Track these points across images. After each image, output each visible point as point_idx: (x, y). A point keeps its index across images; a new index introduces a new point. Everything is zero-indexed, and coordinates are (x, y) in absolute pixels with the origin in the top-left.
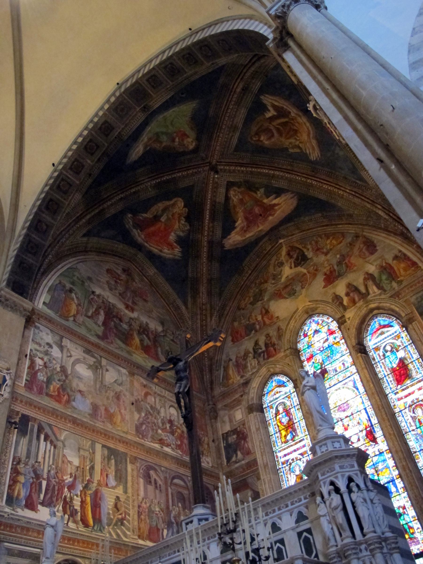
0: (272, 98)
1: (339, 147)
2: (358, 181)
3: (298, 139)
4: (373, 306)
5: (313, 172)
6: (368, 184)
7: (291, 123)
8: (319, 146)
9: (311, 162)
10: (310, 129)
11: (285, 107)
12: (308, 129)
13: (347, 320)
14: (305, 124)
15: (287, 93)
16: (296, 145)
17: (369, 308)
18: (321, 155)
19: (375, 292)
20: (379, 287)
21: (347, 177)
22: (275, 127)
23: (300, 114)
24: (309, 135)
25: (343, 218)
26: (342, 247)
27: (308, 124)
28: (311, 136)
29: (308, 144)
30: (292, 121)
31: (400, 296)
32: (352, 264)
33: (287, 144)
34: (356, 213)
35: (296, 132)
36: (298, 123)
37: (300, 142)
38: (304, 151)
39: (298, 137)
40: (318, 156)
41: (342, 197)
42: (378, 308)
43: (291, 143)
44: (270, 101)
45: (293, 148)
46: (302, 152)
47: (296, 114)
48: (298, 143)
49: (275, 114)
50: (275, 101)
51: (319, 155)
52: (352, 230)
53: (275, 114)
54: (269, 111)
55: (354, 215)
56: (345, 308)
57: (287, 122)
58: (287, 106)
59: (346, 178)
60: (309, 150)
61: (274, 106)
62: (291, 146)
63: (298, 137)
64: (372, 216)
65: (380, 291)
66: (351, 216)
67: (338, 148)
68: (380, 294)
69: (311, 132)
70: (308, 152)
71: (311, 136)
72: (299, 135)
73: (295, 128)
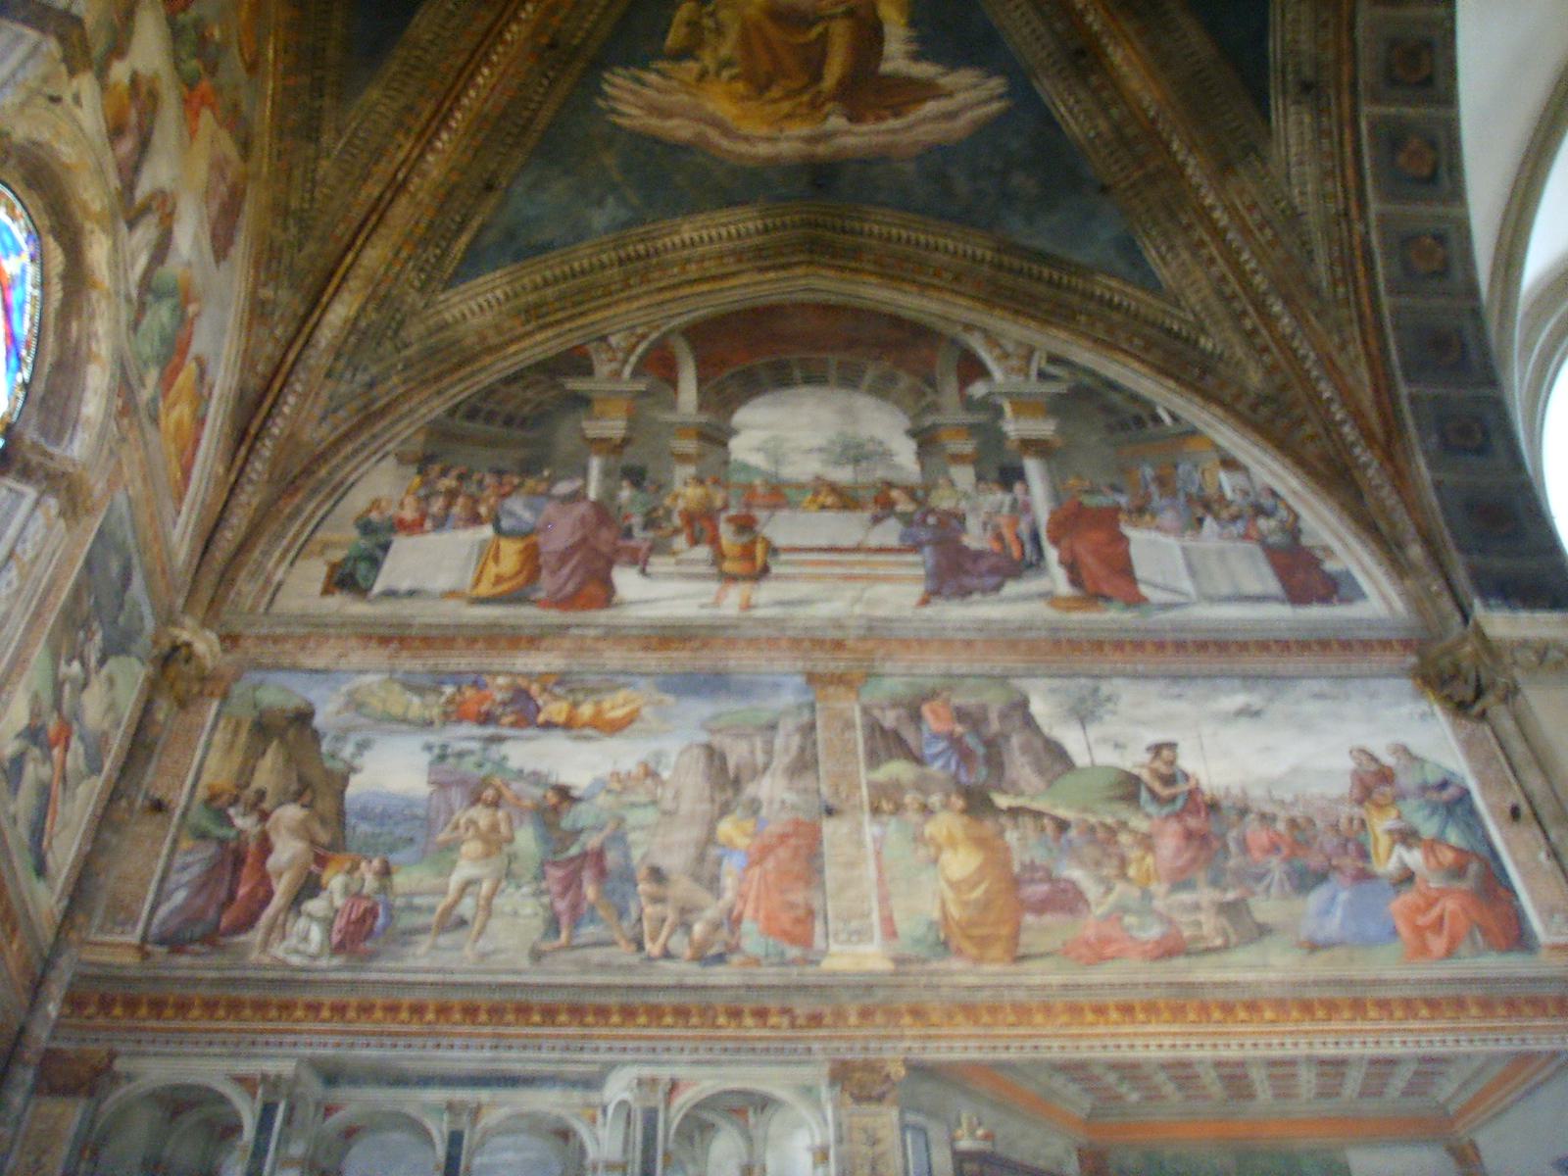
0: (970, 115)
1: (627, 225)
2: (465, 239)
3: (725, 74)
4: (98, 252)
5: (552, 46)
6: (448, 285)
7: (800, 91)
8: (657, 140)
9: (599, 65)
10: (742, 148)
11: (893, 123)
12: (747, 139)
13: (75, 83)
14: (769, 139)
15: (962, 185)
16: (700, 43)
17: (88, 226)
18: (619, 128)
19: (132, 266)
20: (146, 284)
21: (493, 200)
22: (822, 18)
23: (822, 150)
24: (716, 123)
25: (305, 80)
26: (233, 65)
27: (763, 150)
28: (713, 135)
29: (685, 98)
30: (806, 98)
31: (126, 421)
32: (197, 114)
33: (724, 15)
34: (325, 164)
35: (759, 86)
36: (789, 116)
37: (703, 75)
38: (661, 65)
39: (733, 78)
40: (621, 114)
41: (399, 124)
42: (75, 278)
43: (719, 31)
44: (961, 98)
45: (693, 25)
46: (660, 55)
47: (828, 136)
48: (708, 59)
49: (886, 67)
50: (950, 116)
51: (625, 122)
52: (262, 116)
53: (886, 67)
54: (916, 57)
55: (311, 151)
56: (102, 74)
57: (817, 77)
58: (894, 131)
59: (489, 187)
60: (659, 90)
61: (926, 90)
62: (708, 22)
63: (733, 78)
64: (311, 247)
65: (134, 293)
66: (310, 131)
67: (623, 214)
68: (128, 299)
69: (725, 143)
70: (652, 78)
71: (713, 135)
72: (740, 87)
73: (775, 92)
